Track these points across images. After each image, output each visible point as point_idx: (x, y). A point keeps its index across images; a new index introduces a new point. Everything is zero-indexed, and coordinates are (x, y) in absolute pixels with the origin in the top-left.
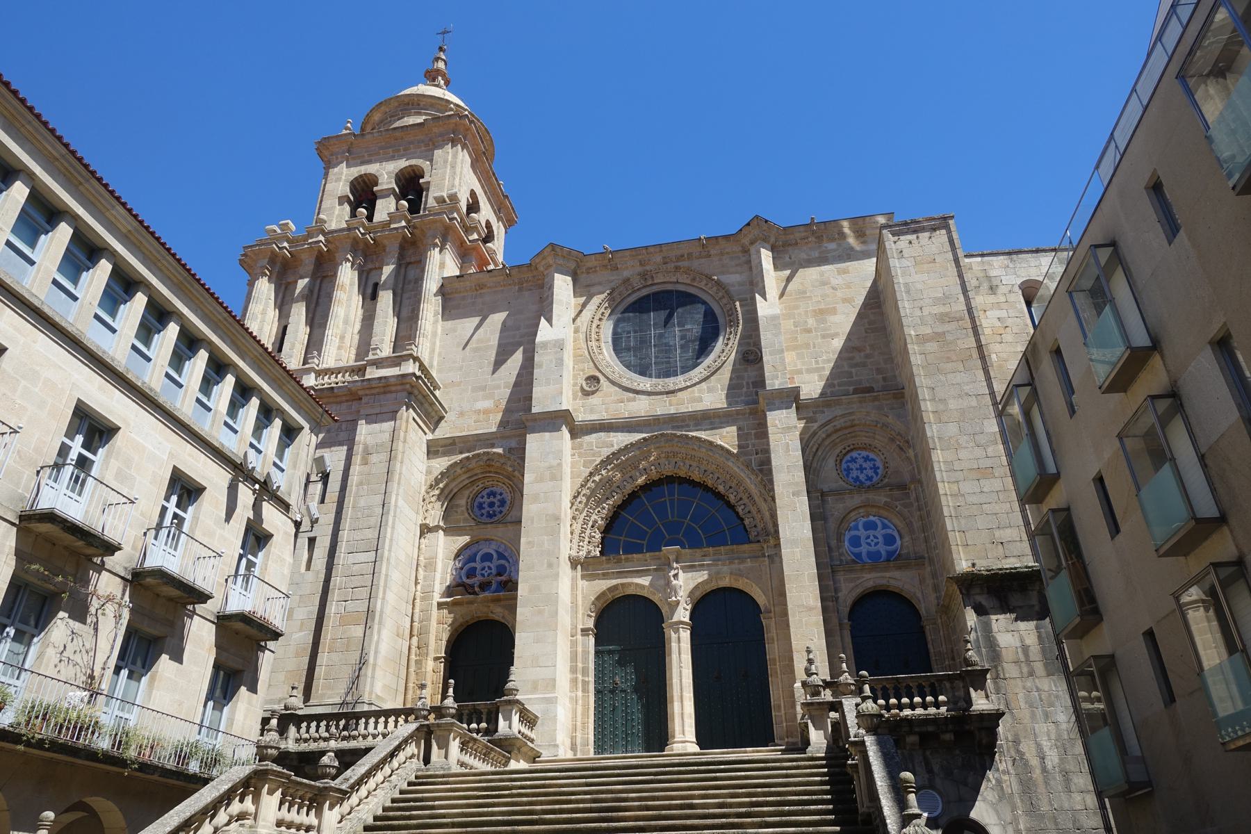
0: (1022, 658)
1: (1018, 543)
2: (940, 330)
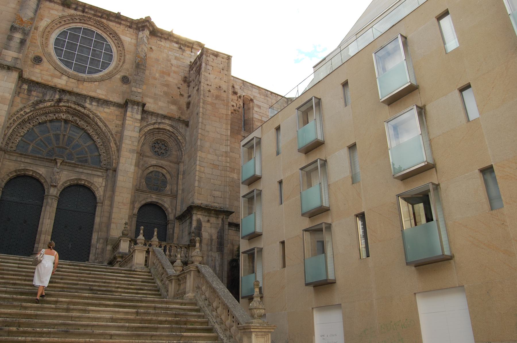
0: (210, 244)
1: (220, 198)
2: (215, 102)
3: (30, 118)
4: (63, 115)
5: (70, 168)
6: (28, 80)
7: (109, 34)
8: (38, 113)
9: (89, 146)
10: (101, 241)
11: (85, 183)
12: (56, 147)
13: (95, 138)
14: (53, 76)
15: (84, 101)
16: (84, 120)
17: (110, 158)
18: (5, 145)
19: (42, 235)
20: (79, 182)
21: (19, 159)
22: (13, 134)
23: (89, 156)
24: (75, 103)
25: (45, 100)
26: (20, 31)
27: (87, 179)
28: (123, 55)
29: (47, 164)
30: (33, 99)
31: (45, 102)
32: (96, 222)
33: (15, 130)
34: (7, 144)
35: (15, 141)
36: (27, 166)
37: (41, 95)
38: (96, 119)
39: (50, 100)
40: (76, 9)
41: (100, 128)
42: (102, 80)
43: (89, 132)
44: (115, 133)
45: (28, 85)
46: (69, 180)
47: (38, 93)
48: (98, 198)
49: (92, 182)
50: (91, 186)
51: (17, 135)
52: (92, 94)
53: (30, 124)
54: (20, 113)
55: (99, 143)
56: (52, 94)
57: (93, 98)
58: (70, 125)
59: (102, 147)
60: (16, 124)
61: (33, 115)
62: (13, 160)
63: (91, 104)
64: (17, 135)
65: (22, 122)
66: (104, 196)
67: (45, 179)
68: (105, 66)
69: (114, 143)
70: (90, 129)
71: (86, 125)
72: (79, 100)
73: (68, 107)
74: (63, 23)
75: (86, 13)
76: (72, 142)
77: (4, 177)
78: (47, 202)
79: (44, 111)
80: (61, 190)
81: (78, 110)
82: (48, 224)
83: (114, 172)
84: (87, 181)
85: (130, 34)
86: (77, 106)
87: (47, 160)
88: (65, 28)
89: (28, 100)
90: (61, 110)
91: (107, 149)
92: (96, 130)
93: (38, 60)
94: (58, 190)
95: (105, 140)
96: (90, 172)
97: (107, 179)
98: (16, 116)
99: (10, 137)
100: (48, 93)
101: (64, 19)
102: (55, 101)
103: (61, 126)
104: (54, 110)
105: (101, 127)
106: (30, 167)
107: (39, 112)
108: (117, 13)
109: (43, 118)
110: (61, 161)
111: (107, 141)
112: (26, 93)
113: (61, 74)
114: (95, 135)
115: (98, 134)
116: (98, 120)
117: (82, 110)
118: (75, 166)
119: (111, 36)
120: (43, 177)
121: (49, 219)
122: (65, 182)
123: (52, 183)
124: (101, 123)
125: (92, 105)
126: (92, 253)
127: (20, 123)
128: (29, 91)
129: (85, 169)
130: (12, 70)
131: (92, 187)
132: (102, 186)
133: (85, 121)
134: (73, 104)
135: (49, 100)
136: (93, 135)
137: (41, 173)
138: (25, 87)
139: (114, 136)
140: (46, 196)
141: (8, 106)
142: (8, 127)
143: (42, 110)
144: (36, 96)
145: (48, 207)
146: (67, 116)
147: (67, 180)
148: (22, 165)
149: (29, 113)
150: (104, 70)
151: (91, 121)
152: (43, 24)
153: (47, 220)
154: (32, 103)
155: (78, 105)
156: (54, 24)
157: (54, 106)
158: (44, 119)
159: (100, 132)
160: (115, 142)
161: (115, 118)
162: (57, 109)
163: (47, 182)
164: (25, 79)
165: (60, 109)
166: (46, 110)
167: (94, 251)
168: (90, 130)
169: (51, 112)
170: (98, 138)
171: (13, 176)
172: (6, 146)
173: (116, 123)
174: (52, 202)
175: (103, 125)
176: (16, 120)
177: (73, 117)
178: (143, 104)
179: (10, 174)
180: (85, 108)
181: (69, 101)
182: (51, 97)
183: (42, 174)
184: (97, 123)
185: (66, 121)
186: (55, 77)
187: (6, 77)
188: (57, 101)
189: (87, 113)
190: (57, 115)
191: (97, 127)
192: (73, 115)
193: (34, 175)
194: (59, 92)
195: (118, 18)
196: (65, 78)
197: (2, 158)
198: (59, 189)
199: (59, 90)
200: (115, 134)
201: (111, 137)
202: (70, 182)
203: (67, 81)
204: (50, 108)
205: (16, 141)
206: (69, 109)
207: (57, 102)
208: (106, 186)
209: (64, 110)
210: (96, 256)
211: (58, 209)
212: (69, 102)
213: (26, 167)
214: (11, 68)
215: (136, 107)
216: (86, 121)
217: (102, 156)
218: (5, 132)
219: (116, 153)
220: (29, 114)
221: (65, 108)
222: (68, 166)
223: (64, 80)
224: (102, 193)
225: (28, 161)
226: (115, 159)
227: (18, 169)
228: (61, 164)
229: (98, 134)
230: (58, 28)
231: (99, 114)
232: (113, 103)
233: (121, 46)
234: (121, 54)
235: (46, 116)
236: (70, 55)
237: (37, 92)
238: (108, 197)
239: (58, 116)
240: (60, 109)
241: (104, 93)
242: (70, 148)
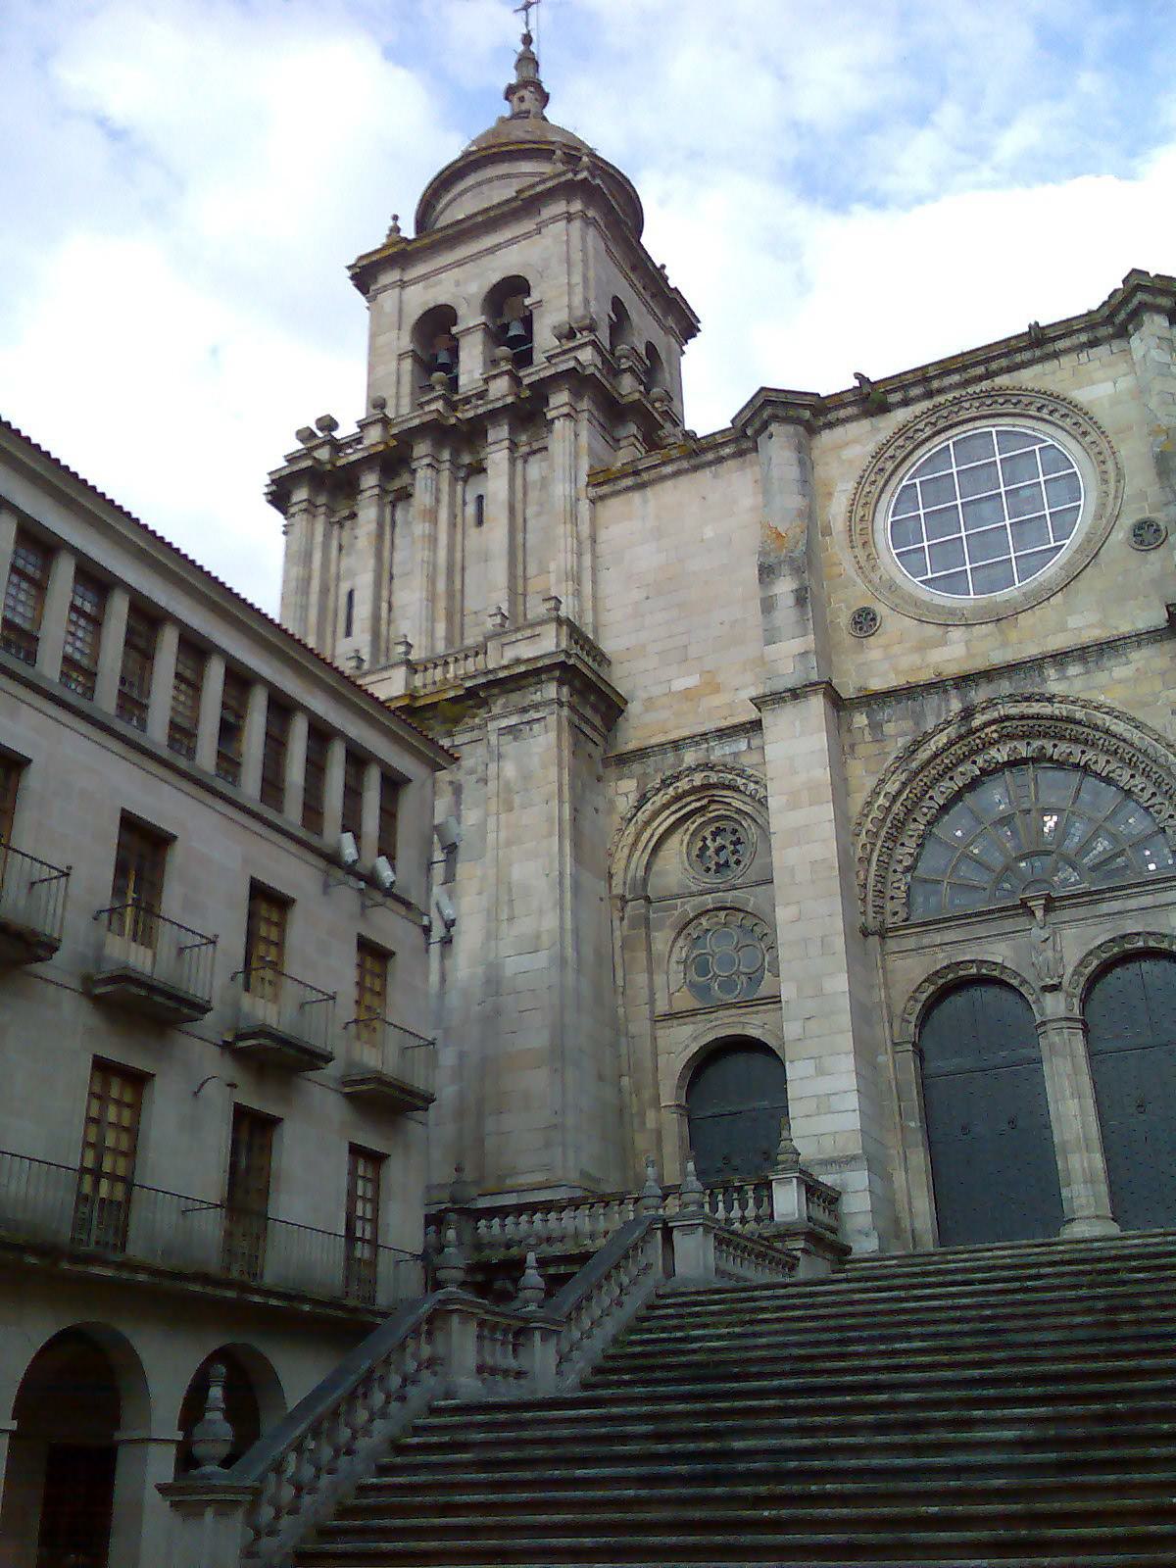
5: (1082, 912)
7: (1038, 414)
13: (1124, 777)
14: (922, 647)
16: (1064, 736)
21: (926, 941)
24: (1013, 698)
26: (785, 569)
27: (1149, 930)
28: (1107, 452)
29: (1008, 925)
30: (897, 745)
33: (881, 859)
37: (911, 723)
38: (1100, 718)
39: (941, 727)
40: (906, 403)
41: (1124, 740)
42: (1071, 579)
43: (1098, 768)
46: (1090, 953)
52: (1057, 642)
55: (1142, 790)
56: (939, 706)
59: (1158, 799)
64: (895, 871)
68: (1063, 522)
70: (1094, 759)
71: (1077, 749)
74: (890, 466)
75: (940, 391)
78: (1052, 1046)
80: (1078, 991)
81: (1033, 718)
85: (1103, 366)
86: (1026, 704)
88: (902, 479)
92: (1116, 752)
93: (865, 621)
94: (1069, 996)
95: (1156, 773)
98: (869, 819)
101: (886, 455)
105: (1127, 735)
106: (965, 954)
108: (1027, 329)
109: (948, 787)
111: (1164, 775)
114: (1118, 771)
115: (1130, 763)
117: (1047, 709)
118: (1093, 897)
119: (1044, 414)
122: (1083, 963)
124: (1122, 724)
125: (1067, 678)
128: (875, 726)
133: (1071, 740)
136: (1114, 771)
138: (861, 720)
148: (941, 956)
149: (899, 792)
150: (1067, 542)
151: (1085, 729)
152: (837, 509)
155: (1027, 699)
156: (867, 489)
157: (961, 737)
161: (1158, 686)
165: (979, 738)
168: (1096, 762)
170: (1133, 776)
172: (880, 918)
177: (1028, 744)
180: (1050, 700)
182: (939, 716)
185: (1013, 764)
187: (797, 723)
189: (1065, 714)
191: (1114, 741)
192: (1026, 736)
193: (984, 971)
194: (957, 687)
195: (1039, 342)
196: (956, 634)
204: (952, 750)
205: (899, 888)
206: (1006, 724)
209: (995, 735)
211: (1092, 1055)
214: (798, 691)
216: (1075, 740)
220: (904, 796)
221: (993, 728)
222: (1075, 905)
223: (958, 643)
230: (882, 491)
231: (1102, 698)
233: (1089, 429)
234: (1100, 453)
235: (951, 778)
236: (947, 552)
239: (985, 761)
240: (979, 738)
241: (1092, 617)
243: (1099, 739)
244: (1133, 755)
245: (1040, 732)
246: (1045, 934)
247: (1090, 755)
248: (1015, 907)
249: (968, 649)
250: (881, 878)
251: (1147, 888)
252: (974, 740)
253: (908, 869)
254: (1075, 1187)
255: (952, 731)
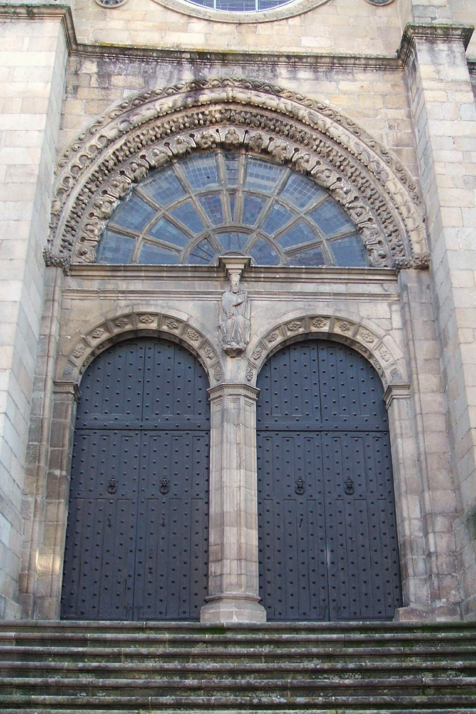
3: (120, 158)
4: (217, 131)
5: (275, 287)
6: (95, 47)
8: (142, 137)
9: (315, 209)
10: (440, 523)
11: (332, 327)
12: (214, 230)
14: (163, 28)
15: (270, 75)
16: (283, 132)
17: (396, 231)
18: (62, 249)
19: (227, 529)
20: (314, 329)
21: (110, 286)
22: (80, 213)
23: (324, 241)
24: (245, 85)
25: (154, 93)
27: (338, 314)
31: (156, 100)
32: (401, 456)
33: (81, 198)
34: (67, 244)
35: (88, 233)
36: (138, 304)
37: (141, 80)
39: (170, 91)
44: (395, 148)
45: (98, 63)
47: (131, 77)
48: (388, 373)
49: (355, 319)
50: (355, 334)
51: (92, 215)
53: (125, 175)
54: (88, 145)
55: (346, 193)
56: (171, 73)
57: (296, 57)
58: (242, 159)
60: (83, 180)
61: (129, 144)
62: (92, 292)
63: (295, 78)
64: (92, 215)
65: (100, 170)
66: (409, 360)
67: (201, 336)
69: (396, 180)
70: (307, 157)
72: (254, 74)
73: (226, 102)
76: (261, 208)
77: (73, 351)
78: (223, 412)
79: (159, 128)
80: (259, 363)
82: (240, 487)
83: (424, 275)
84: (338, 319)
87: (197, 274)
89: (105, 102)
90: (209, 118)
91: (380, 204)
94: (251, 366)
96: (341, 288)
97: (405, 299)
98: (79, 155)
99: (73, 223)
100: (158, 73)
102: (183, 90)
103: (217, 168)
104: (186, 119)
105: (343, 139)
106: (148, 305)
107: (143, 134)
110: (242, 267)
112: (95, 86)
113: (186, 18)
114: (327, 173)
115: (339, 167)
116: (328, 121)
117: (272, 101)
120: (193, 329)
121: (239, 467)
122: (269, 336)
123: (227, 343)
124: (341, 128)
126: (415, 575)
127: (93, 175)
129: (323, 281)
130: (41, 16)
131: (359, 338)
132: (392, 329)
133: (287, 136)
134: (241, 90)
135: (165, 89)
137: (184, 317)
139: (394, 155)
140: (214, 390)
141: (45, 116)
142: (61, 192)
143: (152, 125)
144: (124, 87)
145: (229, 428)
146: (229, 133)
147: (271, 327)
148: (123, 303)
151: (306, 129)
153: (235, 472)
154: (118, 106)
155: (256, 87)
157: (185, 107)
158: (163, 155)
159: (342, 158)
160: (399, 175)
161: (379, 103)
162: (196, 116)
163: (210, 345)
164: (85, 46)
165: (203, 113)
166: (163, 126)
167: (421, 566)
168: (307, 161)
169: (181, 130)
170: (339, 179)
171: (102, 344)
172: (66, 253)
173: (389, 117)
174: (239, 409)
175: (347, 132)
176: (81, 167)
177: (246, 132)
178: (464, 30)
179: (89, 339)
180: (277, 92)
181: (226, 82)
182: (169, 80)
183: (188, 319)
184: (327, 130)
186: (169, 30)
187: (27, 40)
188: (189, 91)
189: (289, 108)
190: (198, 136)
191: (329, 143)
192: (246, 124)
193: (165, 328)
194: (192, 61)
196: (198, 26)
197: (57, 289)
198: (252, 360)
199: (188, 56)
200: (394, 150)
201: (383, 164)
202: (283, 335)
203: (206, 34)
204: (174, 117)
206: (232, 107)
207: (192, 93)
208: (406, 323)
209: (218, 116)
210: (436, 584)
212: (225, 86)
213: (135, 307)
214: (35, 11)
215: (442, 46)
216: (290, 137)
217: (367, 232)
218: (53, 207)
219: (413, 210)
221: (218, 107)
223: (199, 33)
224: (398, 353)
225: (137, 285)
226: (417, 229)
227: (111, 316)
228: (242, 278)
229: (338, 164)
232: (363, 62)
235: (167, 144)
237: (125, 75)
238: (426, 360)
239: (203, 137)
240: (203, 113)
242: (258, 227)
243: (315, 140)
244: (345, 159)
245: (260, 124)
246: (236, 299)
247: (303, 153)
248: (210, 269)
249: (207, 40)
250: (75, 215)
251: (343, 277)
252: (198, 114)
253: (106, 217)
254: (227, 562)
255: (178, 99)
